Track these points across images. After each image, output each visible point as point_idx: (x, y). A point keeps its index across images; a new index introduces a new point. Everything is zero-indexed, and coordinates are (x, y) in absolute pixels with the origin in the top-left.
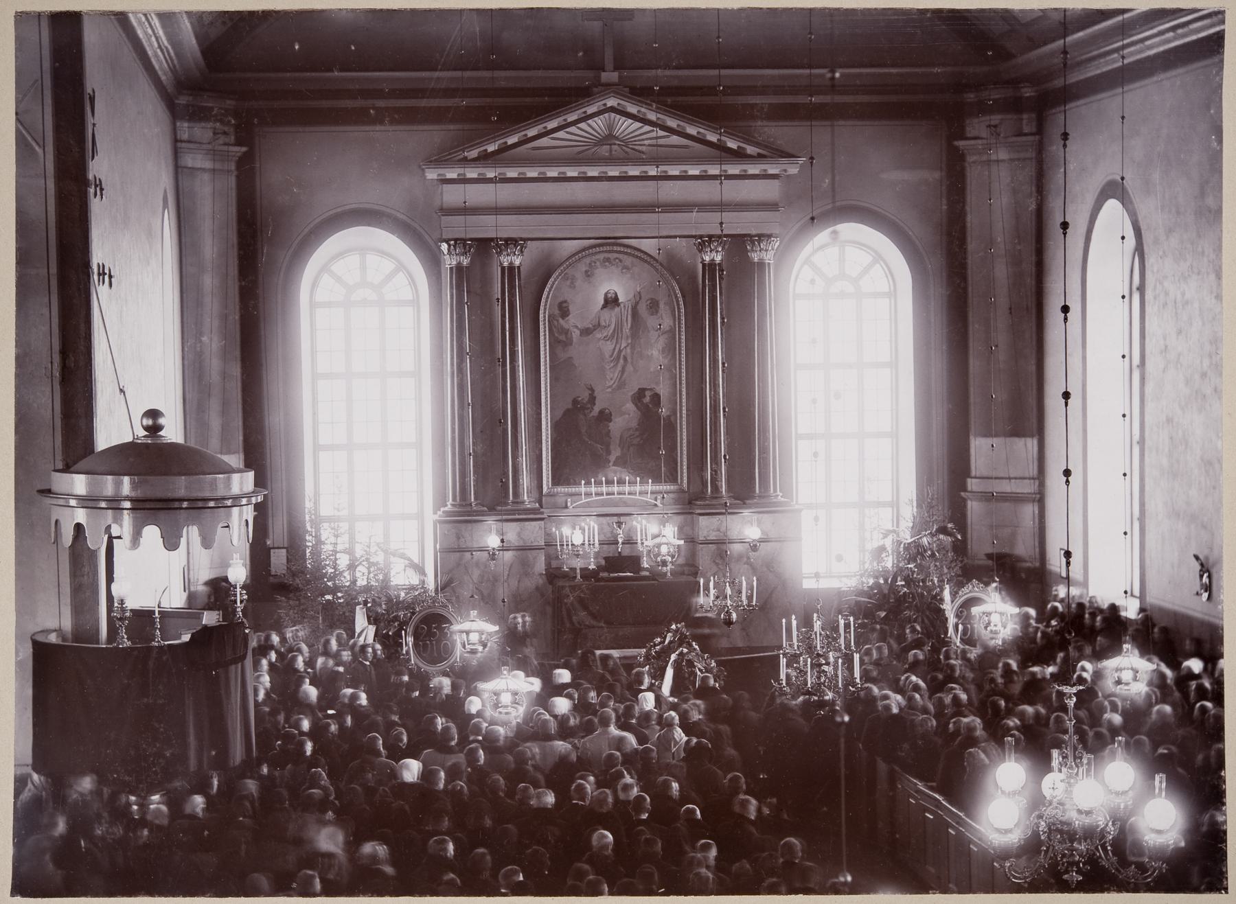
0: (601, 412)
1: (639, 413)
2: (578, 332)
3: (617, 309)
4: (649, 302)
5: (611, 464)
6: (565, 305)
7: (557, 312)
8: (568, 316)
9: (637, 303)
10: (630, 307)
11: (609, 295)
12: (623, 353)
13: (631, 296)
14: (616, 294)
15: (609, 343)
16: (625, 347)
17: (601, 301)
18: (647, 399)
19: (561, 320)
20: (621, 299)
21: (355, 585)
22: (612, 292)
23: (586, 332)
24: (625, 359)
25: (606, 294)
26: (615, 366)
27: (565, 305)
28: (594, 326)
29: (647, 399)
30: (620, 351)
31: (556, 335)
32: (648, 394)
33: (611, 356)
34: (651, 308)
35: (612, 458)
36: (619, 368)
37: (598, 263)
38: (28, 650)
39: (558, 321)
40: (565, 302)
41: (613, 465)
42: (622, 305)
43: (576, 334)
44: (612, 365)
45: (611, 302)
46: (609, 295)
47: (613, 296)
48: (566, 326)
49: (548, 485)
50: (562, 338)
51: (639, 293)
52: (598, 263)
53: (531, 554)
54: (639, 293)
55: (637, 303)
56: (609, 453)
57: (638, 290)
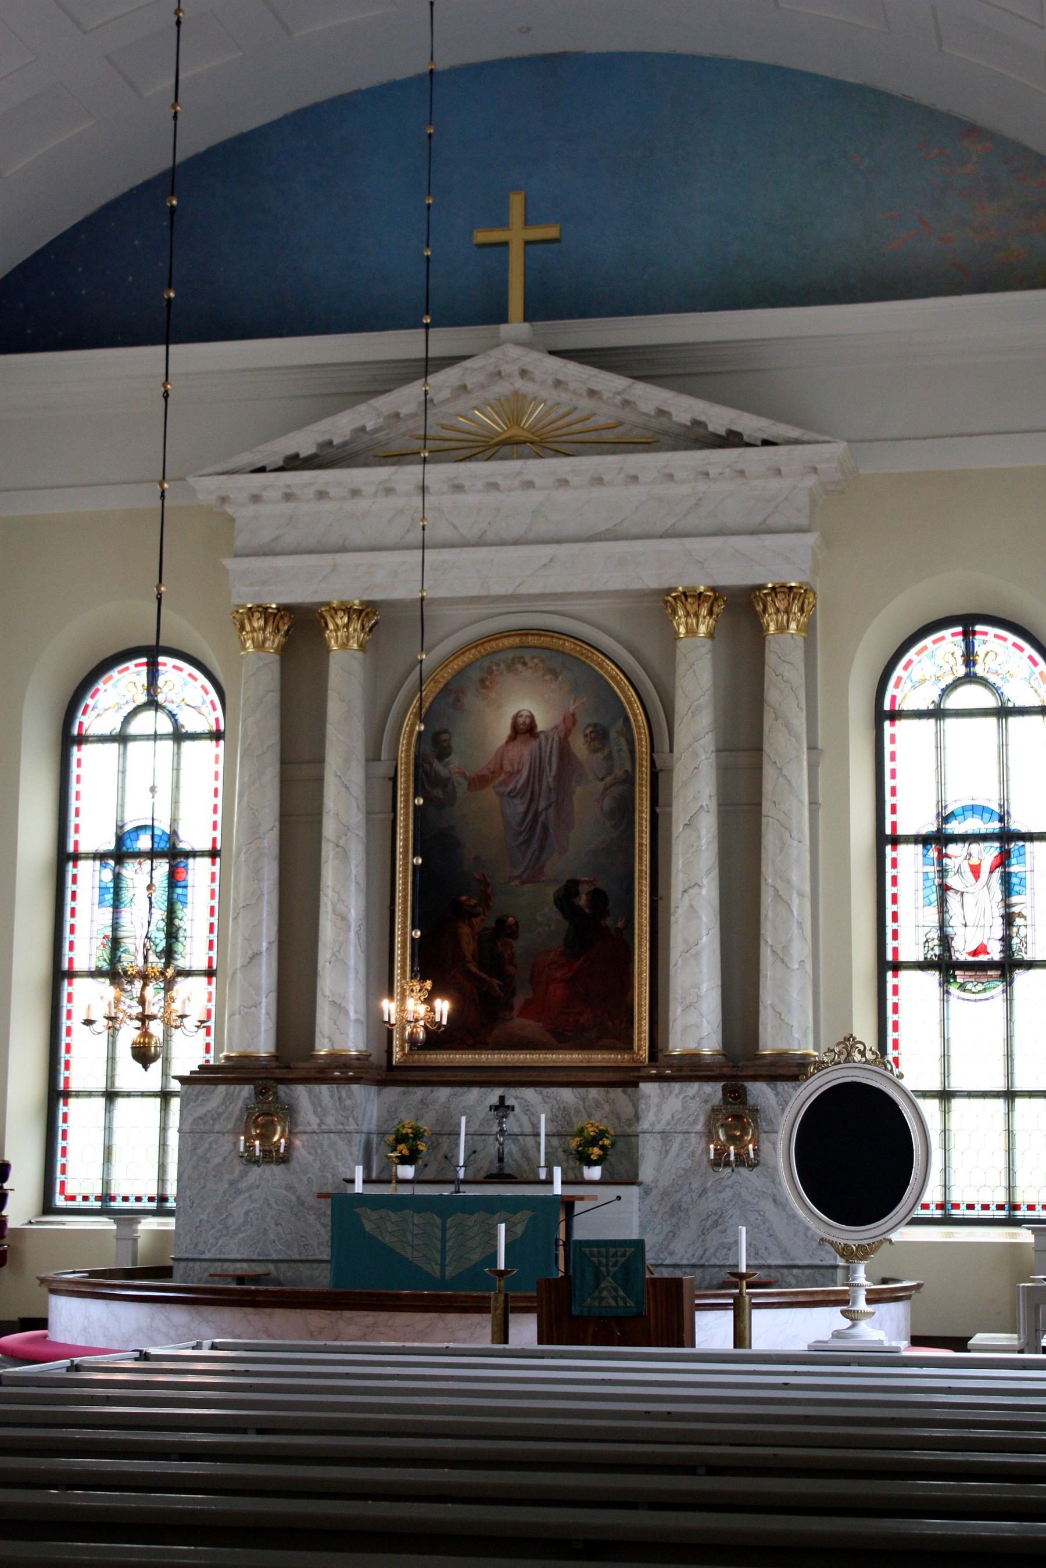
0: (501, 922)
1: (566, 924)
2: (465, 784)
3: (534, 744)
4: (590, 729)
5: (515, 1013)
6: (445, 736)
7: (428, 748)
8: (448, 754)
9: (568, 732)
10: (556, 738)
11: (521, 720)
12: (542, 818)
13: (558, 720)
14: (532, 717)
15: (517, 801)
16: (546, 809)
17: (504, 730)
18: (582, 901)
19: (436, 764)
20: (541, 725)
21: (110, 1201)
22: (525, 713)
23: (479, 782)
24: (545, 828)
26: (528, 842)
27: (445, 736)
28: (493, 772)
29: (582, 901)
30: (536, 815)
31: (428, 788)
32: (584, 889)
33: (521, 824)
34: (593, 740)
35: (518, 1002)
36: (535, 845)
37: (502, 666)
39: (431, 764)
40: (445, 732)
41: (521, 1015)
42: (542, 737)
44: (522, 839)
46: (521, 720)
47: (528, 720)
48: (443, 772)
51: (573, 715)
52: (502, 666)
53: (371, 1136)
54: (573, 715)
55: (568, 732)
57: (571, 709)
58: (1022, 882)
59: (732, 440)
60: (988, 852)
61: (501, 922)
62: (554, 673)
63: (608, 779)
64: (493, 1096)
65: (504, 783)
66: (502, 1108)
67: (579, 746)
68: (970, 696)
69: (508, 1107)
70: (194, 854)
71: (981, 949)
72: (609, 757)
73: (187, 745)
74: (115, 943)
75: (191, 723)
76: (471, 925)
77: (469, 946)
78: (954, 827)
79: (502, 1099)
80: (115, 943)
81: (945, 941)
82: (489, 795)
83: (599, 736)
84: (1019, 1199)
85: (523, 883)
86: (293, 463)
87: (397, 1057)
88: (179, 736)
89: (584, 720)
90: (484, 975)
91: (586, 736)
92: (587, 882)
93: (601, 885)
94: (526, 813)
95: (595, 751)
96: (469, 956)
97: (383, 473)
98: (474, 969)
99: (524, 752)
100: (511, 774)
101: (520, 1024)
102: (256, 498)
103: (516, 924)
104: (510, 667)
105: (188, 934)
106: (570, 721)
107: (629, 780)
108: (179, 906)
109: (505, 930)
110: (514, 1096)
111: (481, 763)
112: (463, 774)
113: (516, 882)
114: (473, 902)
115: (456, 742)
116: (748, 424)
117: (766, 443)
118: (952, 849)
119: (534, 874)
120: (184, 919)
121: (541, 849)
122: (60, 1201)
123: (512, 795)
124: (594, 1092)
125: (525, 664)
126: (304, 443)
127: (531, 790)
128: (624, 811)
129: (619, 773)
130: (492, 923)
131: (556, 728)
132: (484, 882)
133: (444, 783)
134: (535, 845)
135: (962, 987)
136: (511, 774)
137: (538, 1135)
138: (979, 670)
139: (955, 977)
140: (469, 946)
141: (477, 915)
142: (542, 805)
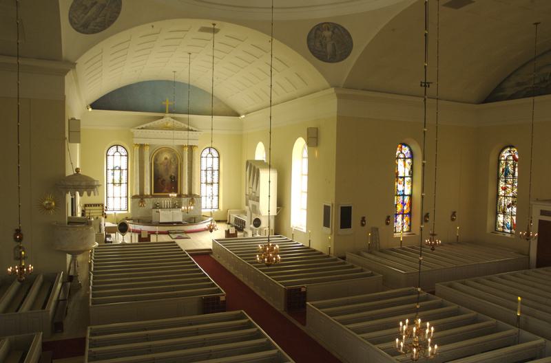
23: (161, 164)
45: (166, 159)
59: (192, 130)
60: (211, 172)
67: (172, 161)
74: (113, 180)
75: (122, 154)
80: (113, 180)
86: (142, 128)
87: (153, 193)
99: (166, 161)
101: (165, 190)
107: (177, 165)
109: (164, 180)
116: (194, 129)
119: (168, 174)
126: (144, 126)
128: (177, 168)
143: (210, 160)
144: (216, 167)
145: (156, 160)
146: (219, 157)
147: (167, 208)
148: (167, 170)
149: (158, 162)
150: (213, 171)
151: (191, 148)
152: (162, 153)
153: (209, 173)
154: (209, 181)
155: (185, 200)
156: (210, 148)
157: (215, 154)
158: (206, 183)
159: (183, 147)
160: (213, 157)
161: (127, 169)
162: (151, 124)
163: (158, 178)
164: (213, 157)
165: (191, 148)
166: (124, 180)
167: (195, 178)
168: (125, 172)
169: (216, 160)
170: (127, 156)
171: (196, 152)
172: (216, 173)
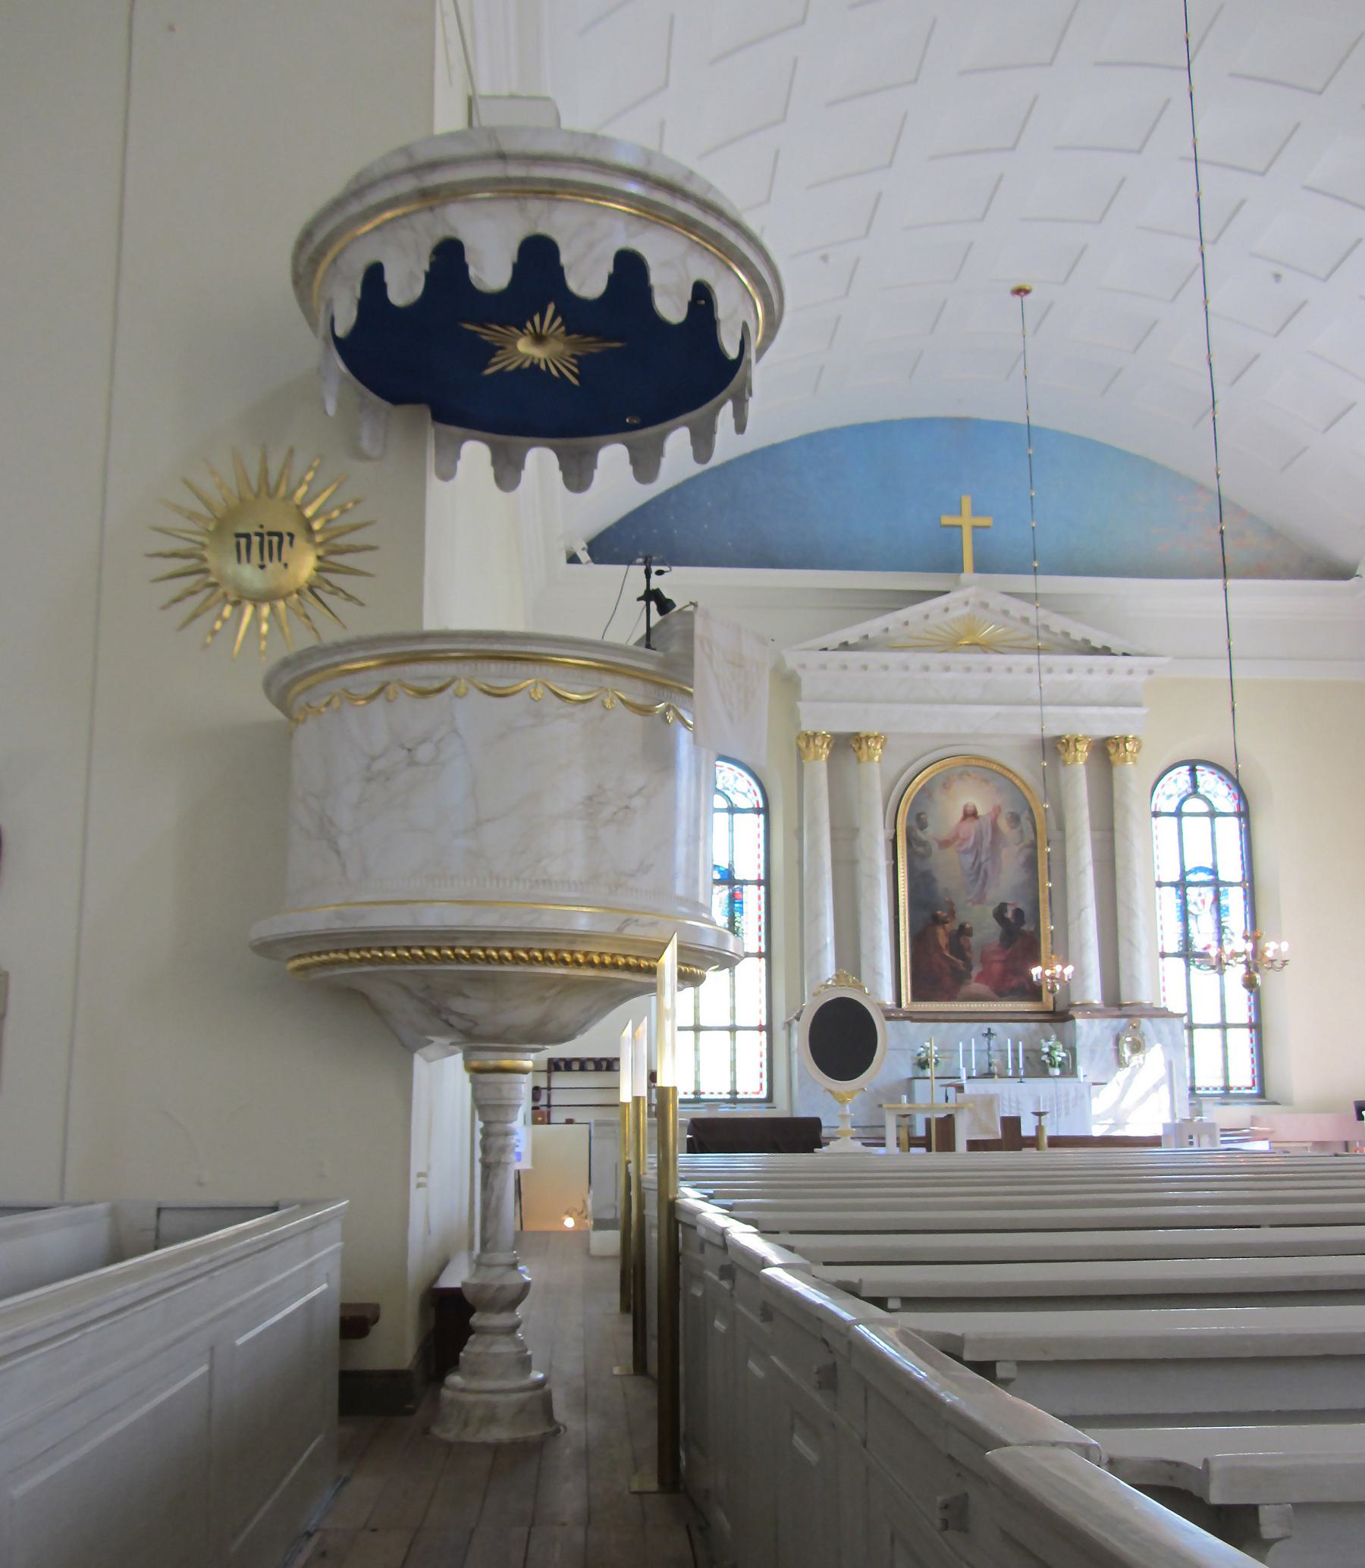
0: (962, 927)
7: (914, 824)
8: (925, 828)
11: (968, 809)
12: (983, 867)
16: (986, 860)
17: (959, 814)
18: (1009, 915)
20: (980, 812)
23: (945, 844)
25: (965, 807)
26: (976, 880)
27: (922, 816)
29: (1009, 915)
30: (980, 865)
35: (974, 973)
36: (980, 882)
38: (1073, 948)
43: (935, 847)
45: (970, 815)
47: (973, 809)
49: (907, 1000)
50: (921, 850)
56: (970, 968)
58: (1227, 909)
59: (1106, 651)
60: (1208, 893)
61: (962, 927)
62: (986, 781)
63: (1022, 845)
64: (984, 1027)
65: (960, 845)
66: (989, 1034)
67: (1003, 824)
68: (1193, 805)
69: (993, 1034)
70: (745, 883)
71: (1207, 947)
72: (1021, 832)
73: (736, 816)
76: (944, 928)
77: (943, 940)
78: (1191, 878)
79: (989, 1029)
81: (1187, 940)
82: (951, 852)
83: (1015, 819)
84: (1231, 1084)
85: (974, 904)
86: (845, 646)
87: (904, 1005)
88: (732, 810)
89: (1006, 810)
90: (954, 958)
91: (1007, 819)
92: (1011, 904)
93: (1020, 906)
94: (974, 863)
95: (1013, 828)
96: (944, 947)
97: (903, 656)
98: (947, 954)
100: (965, 840)
101: (975, 986)
102: (824, 667)
103: (971, 928)
104: (961, 776)
105: (744, 932)
106: (997, 810)
108: (737, 914)
109: (963, 931)
110: (995, 1027)
111: (945, 833)
112: (936, 839)
113: (970, 904)
114: (945, 914)
115: (930, 821)
116: (1114, 643)
117: (1125, 654)
118: (1189, 890)
119: (981, 899)
120: (742, 922)
121: (984, 883)
122: (763, 1095)
123: (965, 852)
124: (1033, 1025)
125: (969, 775)
126: (852, 635)
127: (976, 849)
129: (1027, 841)
130: (956, 927)
131: (988, 814)
132: (952, 904)
133: (924, 844)
134: (980, 882)
135: (1198, 967)
136: (964, 840)
137: (971, 1050)
138: (1201, 790)
139: (1194, 962)
140: (943, 940)
141: (947, 922)
142: (983, 858)
143: (1196, 829)
144: (1231, 869)
145: (918, 820)
146: (1244, 814)
147: (989, 1075)
148: (979, 874)
149: (928, 834)
150: (1217, 884)
151: (1105, 751)
152: (946, 786)
153: (1200, 898)
154: (1203, 936)
155: (1088, 1031)
156: (1193, 766)
157: (1223, 798)
158: (1187, 952)
159: (1054, 748)
160: (1213, 814)
161: (766, 882)
162: (874, 626)
163: (937, 920)
164: (1213, 814)
165: (1105, 751)
166: (752, 937)
167: (1132, 914)
168: (753, 898)
169: (1230, 829)
170: (765, 810)
171: (1132, 774)
172: (1234, 899)
